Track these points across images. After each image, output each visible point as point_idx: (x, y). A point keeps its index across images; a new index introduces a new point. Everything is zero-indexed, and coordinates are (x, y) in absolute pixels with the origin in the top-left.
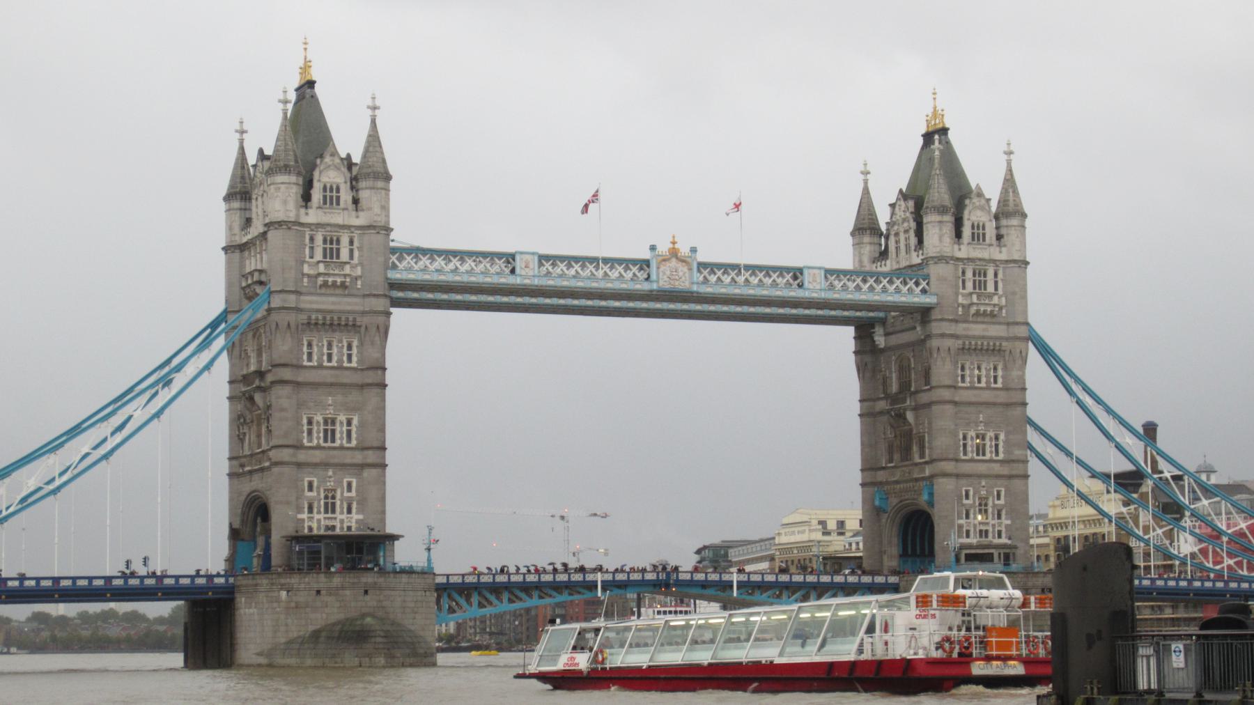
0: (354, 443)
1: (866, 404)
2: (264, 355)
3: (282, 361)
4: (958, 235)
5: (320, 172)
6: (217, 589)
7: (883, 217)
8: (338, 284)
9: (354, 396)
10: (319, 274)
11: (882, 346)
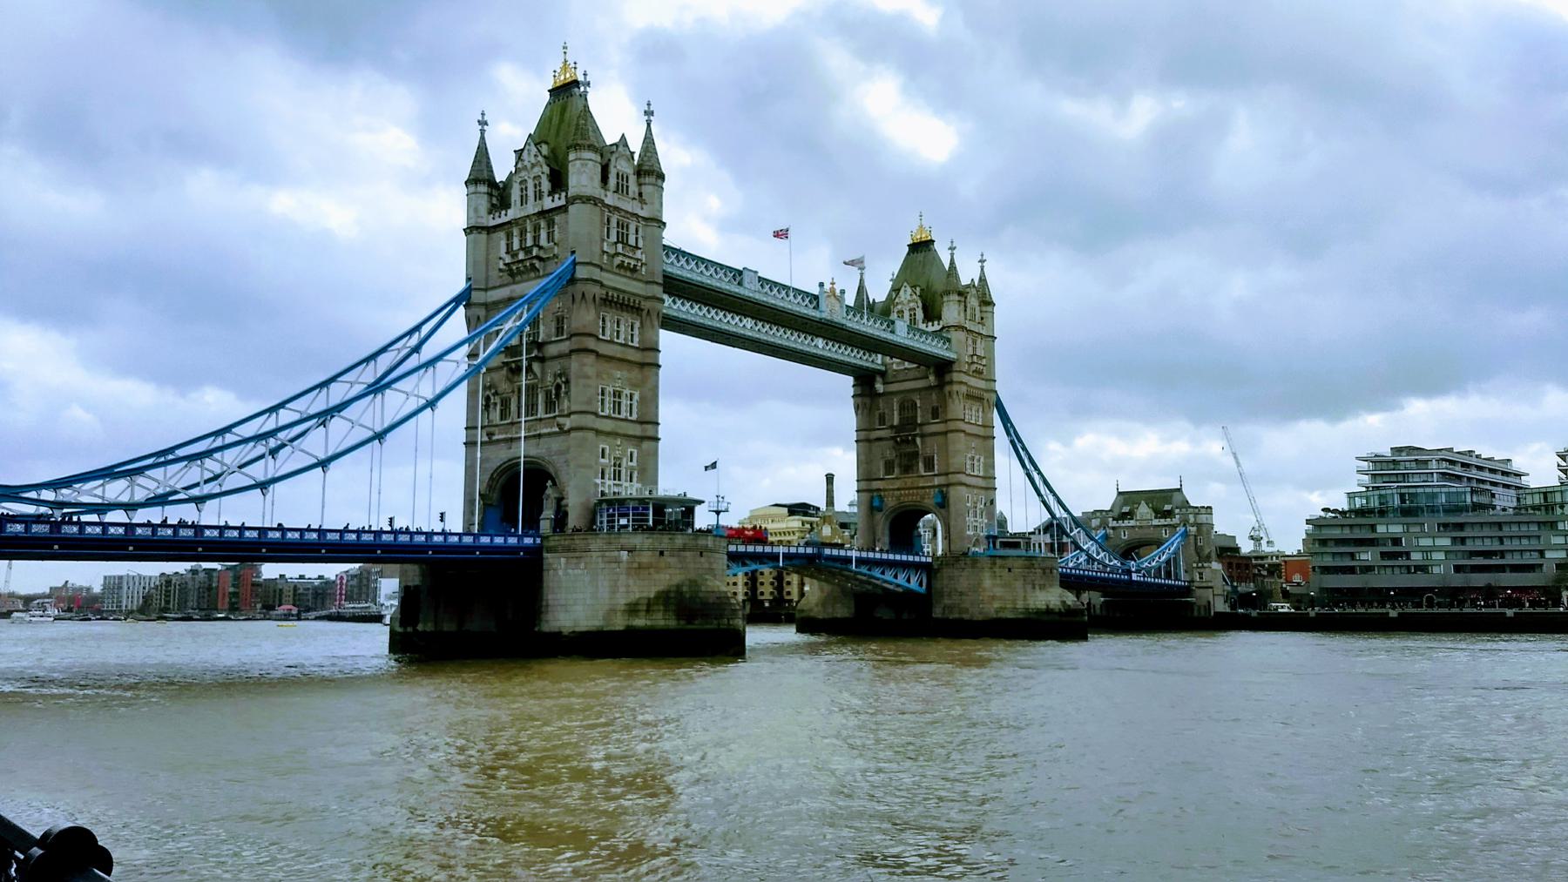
0: (634, 417)
1: (864, 433)
2: (542, 327)
3: (587, 331)
4: (965, 310)
5: (616, 159)
6: (527, 549)
7: (871, 302)
8: (632, 266)
9: (635, 374)
10: (617, 254)
11: (882, 391)
